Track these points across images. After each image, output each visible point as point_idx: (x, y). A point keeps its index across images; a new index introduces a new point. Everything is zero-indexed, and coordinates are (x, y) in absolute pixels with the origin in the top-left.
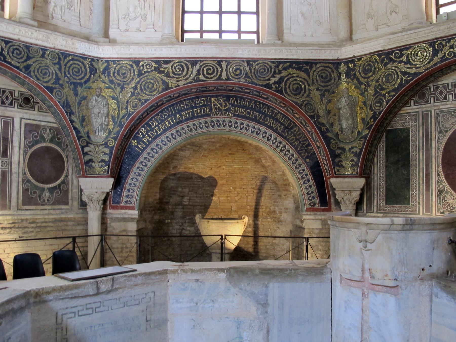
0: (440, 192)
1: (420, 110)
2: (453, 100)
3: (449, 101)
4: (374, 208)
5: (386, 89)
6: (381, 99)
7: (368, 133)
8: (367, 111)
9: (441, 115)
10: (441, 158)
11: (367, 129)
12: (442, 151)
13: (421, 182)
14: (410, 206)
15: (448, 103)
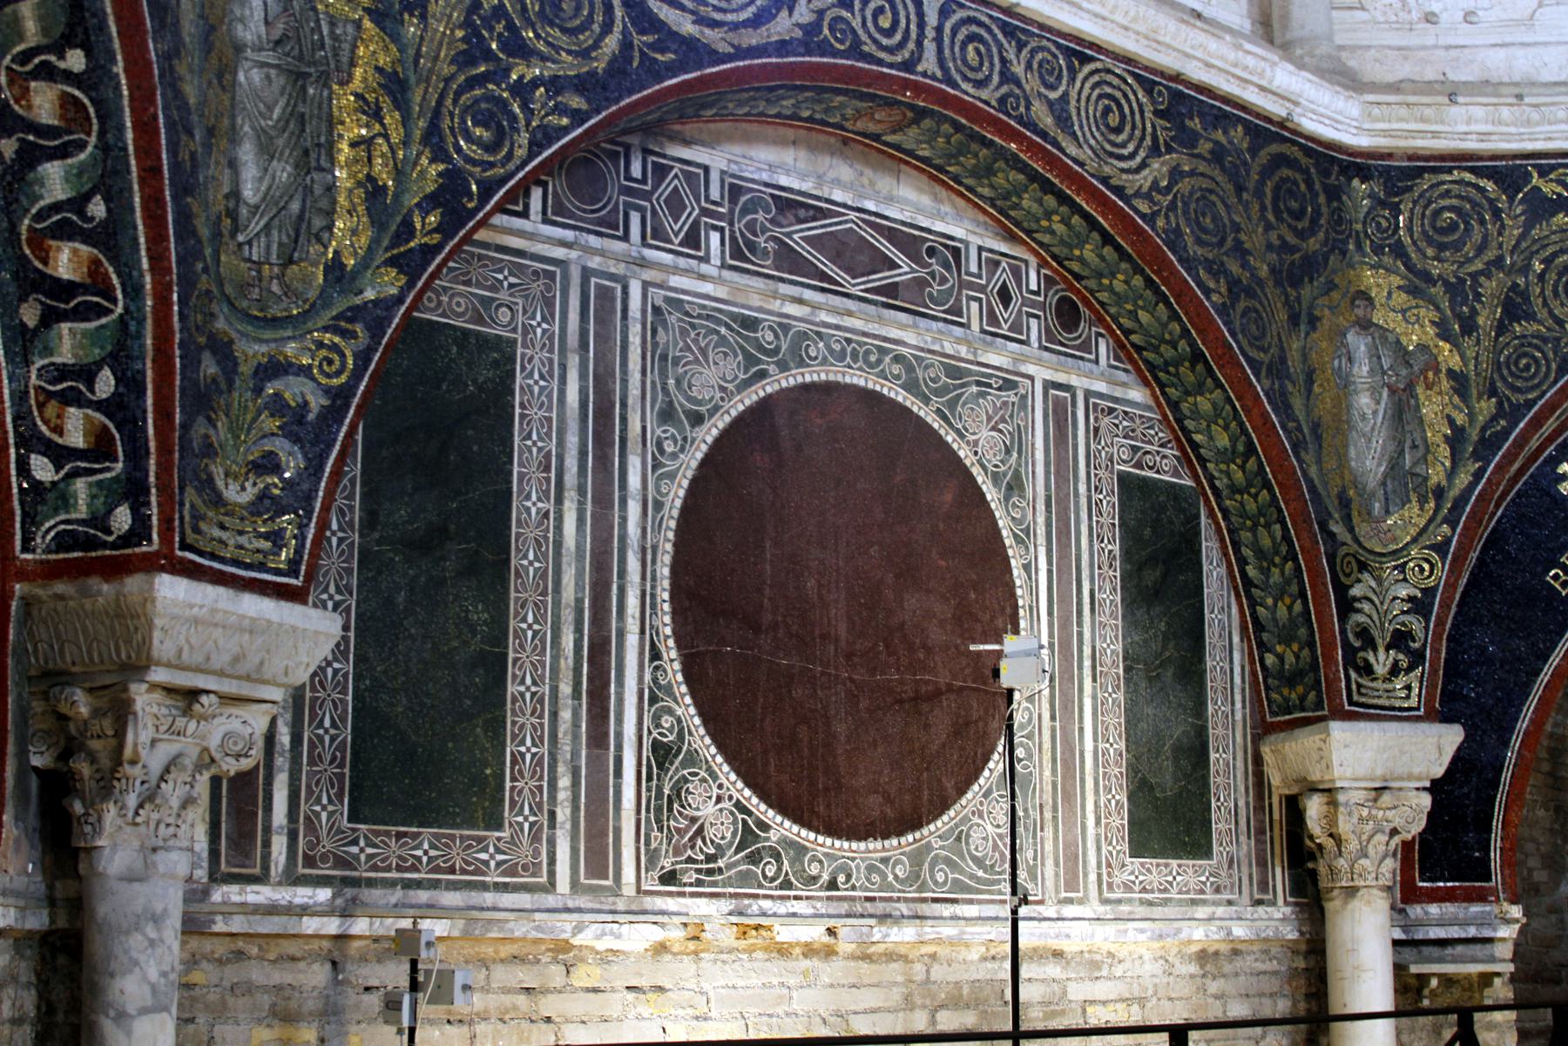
0: (663, 754)
1: (574, 254)
2: (723, 266)
3: (706, 259)
4: (267, 844)
5: (544, 58)
6: (504, 104)
7: (400, 300)
8: (406, 143)
9: (673, 319)
10: (667, 559)
11: (392, 262)
12: (673, 524)
13: (566, 689)
14: (505, 834)
15: (704, 268)
